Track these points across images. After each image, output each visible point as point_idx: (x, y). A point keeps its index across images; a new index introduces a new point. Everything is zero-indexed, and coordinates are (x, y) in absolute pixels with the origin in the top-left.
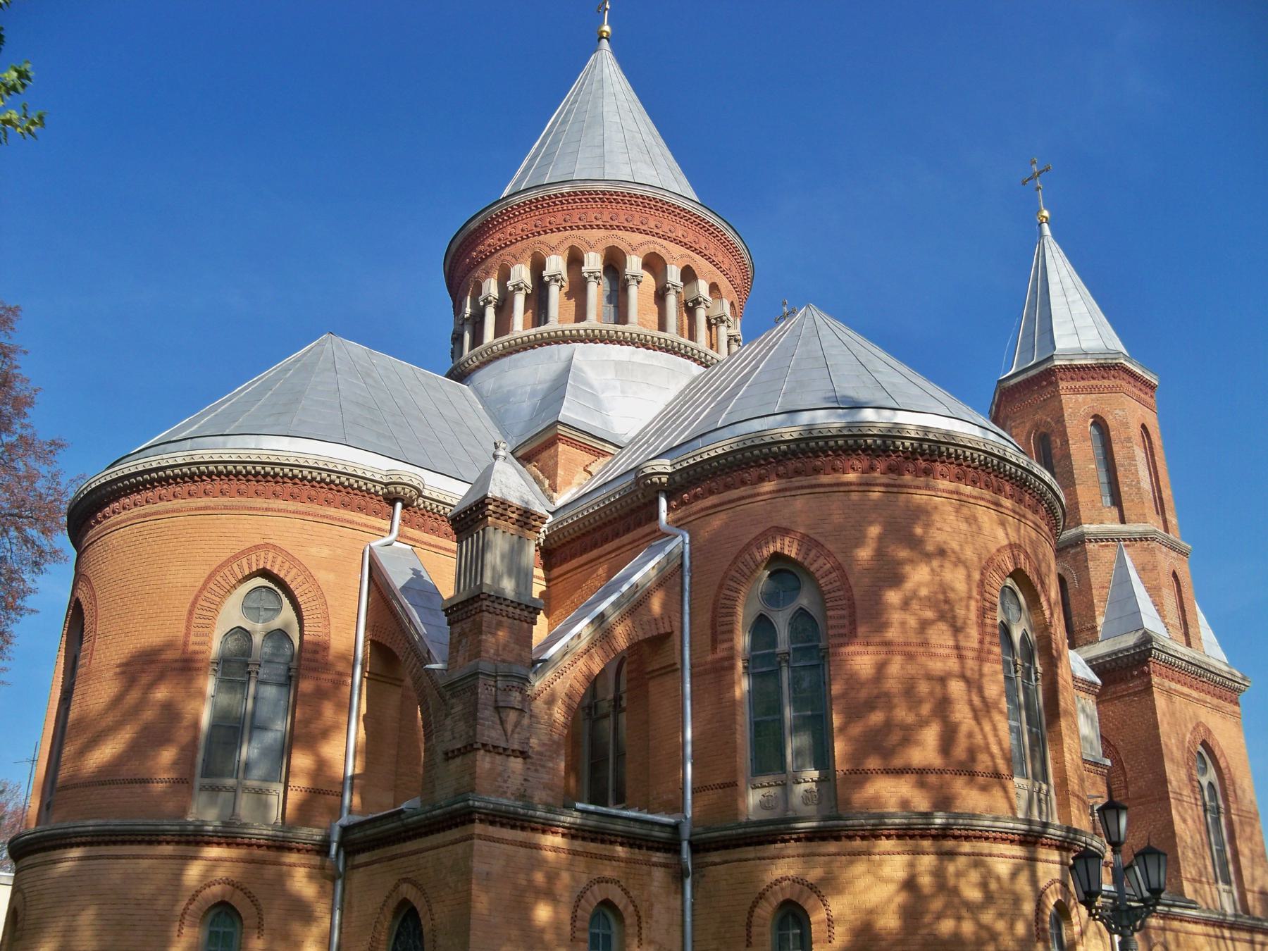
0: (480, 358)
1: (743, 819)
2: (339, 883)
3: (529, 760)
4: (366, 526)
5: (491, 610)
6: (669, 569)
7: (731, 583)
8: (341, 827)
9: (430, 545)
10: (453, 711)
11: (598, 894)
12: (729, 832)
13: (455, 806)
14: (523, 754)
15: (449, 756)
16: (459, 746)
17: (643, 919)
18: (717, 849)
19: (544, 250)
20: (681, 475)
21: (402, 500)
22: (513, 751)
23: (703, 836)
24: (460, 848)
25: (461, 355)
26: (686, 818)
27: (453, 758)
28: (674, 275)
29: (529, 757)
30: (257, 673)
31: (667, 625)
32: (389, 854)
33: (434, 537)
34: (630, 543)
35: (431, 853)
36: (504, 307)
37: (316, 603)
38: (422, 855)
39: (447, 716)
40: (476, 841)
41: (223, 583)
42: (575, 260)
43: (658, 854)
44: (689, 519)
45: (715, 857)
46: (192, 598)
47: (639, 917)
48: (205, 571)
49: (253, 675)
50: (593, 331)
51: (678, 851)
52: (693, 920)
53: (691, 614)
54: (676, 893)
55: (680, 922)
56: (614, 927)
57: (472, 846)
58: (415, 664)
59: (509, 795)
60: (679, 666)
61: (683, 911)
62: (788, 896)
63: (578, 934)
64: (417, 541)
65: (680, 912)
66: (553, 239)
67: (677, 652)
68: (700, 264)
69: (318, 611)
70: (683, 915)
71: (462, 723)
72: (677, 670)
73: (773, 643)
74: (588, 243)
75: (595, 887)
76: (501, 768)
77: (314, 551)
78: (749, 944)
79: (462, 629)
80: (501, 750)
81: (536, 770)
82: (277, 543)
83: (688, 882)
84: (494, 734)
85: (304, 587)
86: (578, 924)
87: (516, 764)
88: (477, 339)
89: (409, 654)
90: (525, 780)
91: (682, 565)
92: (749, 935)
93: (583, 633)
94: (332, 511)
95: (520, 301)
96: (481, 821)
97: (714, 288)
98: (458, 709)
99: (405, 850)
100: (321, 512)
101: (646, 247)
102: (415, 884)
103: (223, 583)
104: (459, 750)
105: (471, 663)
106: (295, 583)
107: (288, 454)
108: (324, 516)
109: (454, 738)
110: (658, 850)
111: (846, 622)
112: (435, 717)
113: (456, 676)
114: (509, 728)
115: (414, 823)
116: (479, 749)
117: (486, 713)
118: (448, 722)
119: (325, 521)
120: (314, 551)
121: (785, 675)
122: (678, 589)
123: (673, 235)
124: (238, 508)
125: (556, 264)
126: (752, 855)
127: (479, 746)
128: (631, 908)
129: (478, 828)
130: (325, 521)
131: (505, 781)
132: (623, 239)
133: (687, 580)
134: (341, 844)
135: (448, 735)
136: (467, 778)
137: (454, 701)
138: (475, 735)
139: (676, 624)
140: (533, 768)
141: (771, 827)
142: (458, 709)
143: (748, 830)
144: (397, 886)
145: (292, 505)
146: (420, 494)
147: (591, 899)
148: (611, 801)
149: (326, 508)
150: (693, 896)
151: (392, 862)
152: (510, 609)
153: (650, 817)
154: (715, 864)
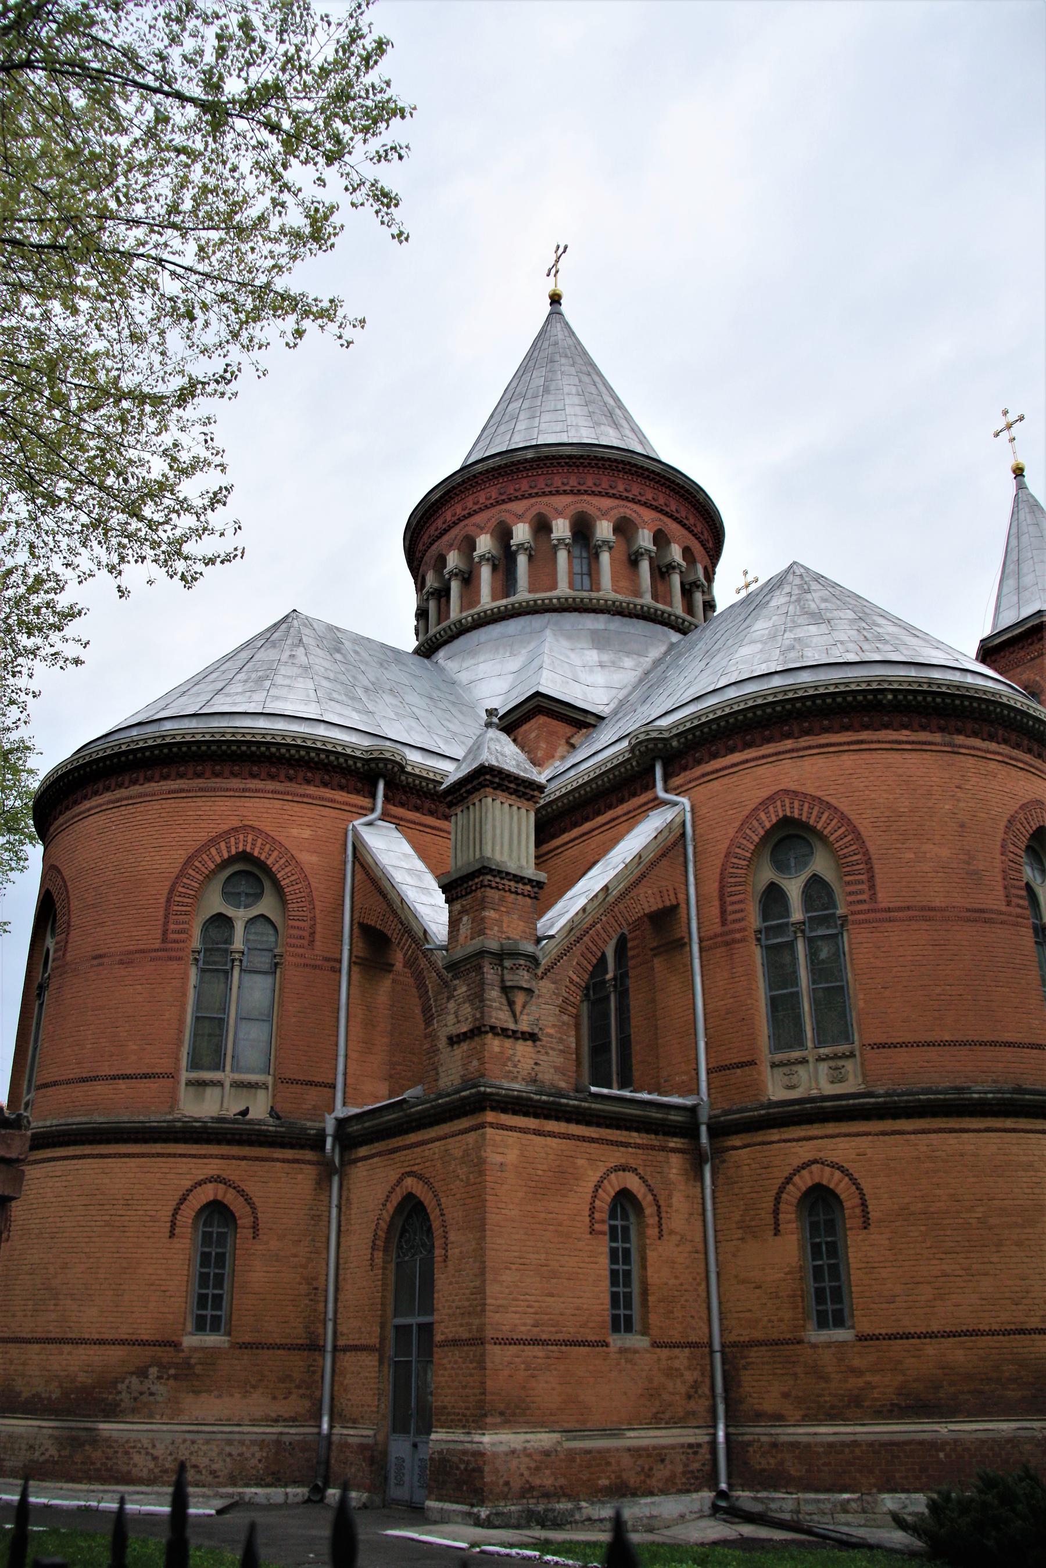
0: (449, 632)
1: (764, 1100)
2: (336, 1179)
3: (538, 1043)
4: (347, 804)
5: (494, 884)
6: (672, 838)
7: (737, 850)
8: (336, 1119)
9: (414, 823)
10: (455, 993)
12: (751, 1114)
13: (463, 1094)
14: (531, 1037)
15: (454, 1041)
16: (464, 1029)
17: (663, 1209)
19: (509, 519)
20: (678, 741)
21: (384, 777)
22: (523, 1033)
23: (722, 1119)
24: (471, 1137)
25: (448, 617)
26: (702, 1100)
27: (458, 1043)
28: (645, 539)
29: (539, 1040)
30: (241, 961)
31: (672, 896)
32: (390, 1147)
33: (418, 815)
34: (625, 814)
35: (438, 1143)
36: (469, 579)
37: (299, 886)
38: (430, 1146)
39: (449, 999)
40: (489, 1130)
41: (203, 869)
42: (542, 527)
43: (675, 1139)
44: (691, 785)
45: (736, 1141)
46: (168, 884)
47: (659, 1207)
48: (181, 856)
49: (237, 963)
50: (566, 599)
51: (696, 1136)
52: (714, 1209)
53: (697, 885)
54: (695, 1180)
55: (700, 1211)
56: (632, 1219)
57: (484, 1134)
58: (410, 946)
59: (520, 1078)
60: (686, 940)
61: (703, 1198)
62: (817, 1180)
63: (597, 1226)
64: (401, 819)
65: (700, 1201)
66: (518, 507)
67: (684, 925)
68: (673, 528)
69: (303, 894)
70: (703, 1204)
71: (467, 1005)
72: (685, 944)
73: (786, 912)
74: (556, 509)
75: (613, 1176)
76: (511, 1052)
77: (295, 832)
78: (777, 1232)
79: (463, 906)
80: (510, 1033)
81: (547, 1053)
82: (255, 824)
85: (287, 870)
86: (597, 1215)
87: (523, 1050)
88: (443, 613)
89: (403, 935)
90: (536, 1064)
91: (683, 835)
92: (777, 1224)
93: (588, 907)
94: (311, 790)
95: (485, 572)
96: (493, 1109)
97: (687, 552)
98: (462, 990)
99: (408, 1142)
100: (301, 791)
101: (616, 511)
102: (420, 1177)
103: (203, 869)
104: (465, 1033)
105: (474, 941)
106: (277, 866)
107: (264, 731)
108: (304, 796)
109: (459, 1022)
110: (675, 1135)
111: (864, 887)
112: (435, 1001)
113: (459, 953)
114: (518, 1008)
115: (418, 1112)
116: (487, 1032)
117: (494, 994)
118: (451, 1005)
119: (305, 800)
120: (295, 832)
121: (801, 947)
122: (681, 859)
123: (643, 499)
124: (214, 790)
125: (521, 533)
126: (776, 1138)
127: (488, 1029)
128: (650, 1197)
129: (490, 1116)
130: (305, 800)
131: (515, 1066)
132: (591, 504)
133: (690, 850)
134: (336, 1137)
135: (451, 1019)
136: (475, 1063)
137: (456, 982)
138: (482, 1017)
139: (682, 897)
140: (543, 1051)
141: (797, 1107)
142: (462, 990)
143: (771, 1111)
144: (400, 1181)
145: (271, 785)
146: (402, 768)
147: (609, 1188)
148: (615, 1084)
149: (306, 787)
150: (713, 1183)
151: (393, 1156)
152: (512, 884)
153: (665, 1099)
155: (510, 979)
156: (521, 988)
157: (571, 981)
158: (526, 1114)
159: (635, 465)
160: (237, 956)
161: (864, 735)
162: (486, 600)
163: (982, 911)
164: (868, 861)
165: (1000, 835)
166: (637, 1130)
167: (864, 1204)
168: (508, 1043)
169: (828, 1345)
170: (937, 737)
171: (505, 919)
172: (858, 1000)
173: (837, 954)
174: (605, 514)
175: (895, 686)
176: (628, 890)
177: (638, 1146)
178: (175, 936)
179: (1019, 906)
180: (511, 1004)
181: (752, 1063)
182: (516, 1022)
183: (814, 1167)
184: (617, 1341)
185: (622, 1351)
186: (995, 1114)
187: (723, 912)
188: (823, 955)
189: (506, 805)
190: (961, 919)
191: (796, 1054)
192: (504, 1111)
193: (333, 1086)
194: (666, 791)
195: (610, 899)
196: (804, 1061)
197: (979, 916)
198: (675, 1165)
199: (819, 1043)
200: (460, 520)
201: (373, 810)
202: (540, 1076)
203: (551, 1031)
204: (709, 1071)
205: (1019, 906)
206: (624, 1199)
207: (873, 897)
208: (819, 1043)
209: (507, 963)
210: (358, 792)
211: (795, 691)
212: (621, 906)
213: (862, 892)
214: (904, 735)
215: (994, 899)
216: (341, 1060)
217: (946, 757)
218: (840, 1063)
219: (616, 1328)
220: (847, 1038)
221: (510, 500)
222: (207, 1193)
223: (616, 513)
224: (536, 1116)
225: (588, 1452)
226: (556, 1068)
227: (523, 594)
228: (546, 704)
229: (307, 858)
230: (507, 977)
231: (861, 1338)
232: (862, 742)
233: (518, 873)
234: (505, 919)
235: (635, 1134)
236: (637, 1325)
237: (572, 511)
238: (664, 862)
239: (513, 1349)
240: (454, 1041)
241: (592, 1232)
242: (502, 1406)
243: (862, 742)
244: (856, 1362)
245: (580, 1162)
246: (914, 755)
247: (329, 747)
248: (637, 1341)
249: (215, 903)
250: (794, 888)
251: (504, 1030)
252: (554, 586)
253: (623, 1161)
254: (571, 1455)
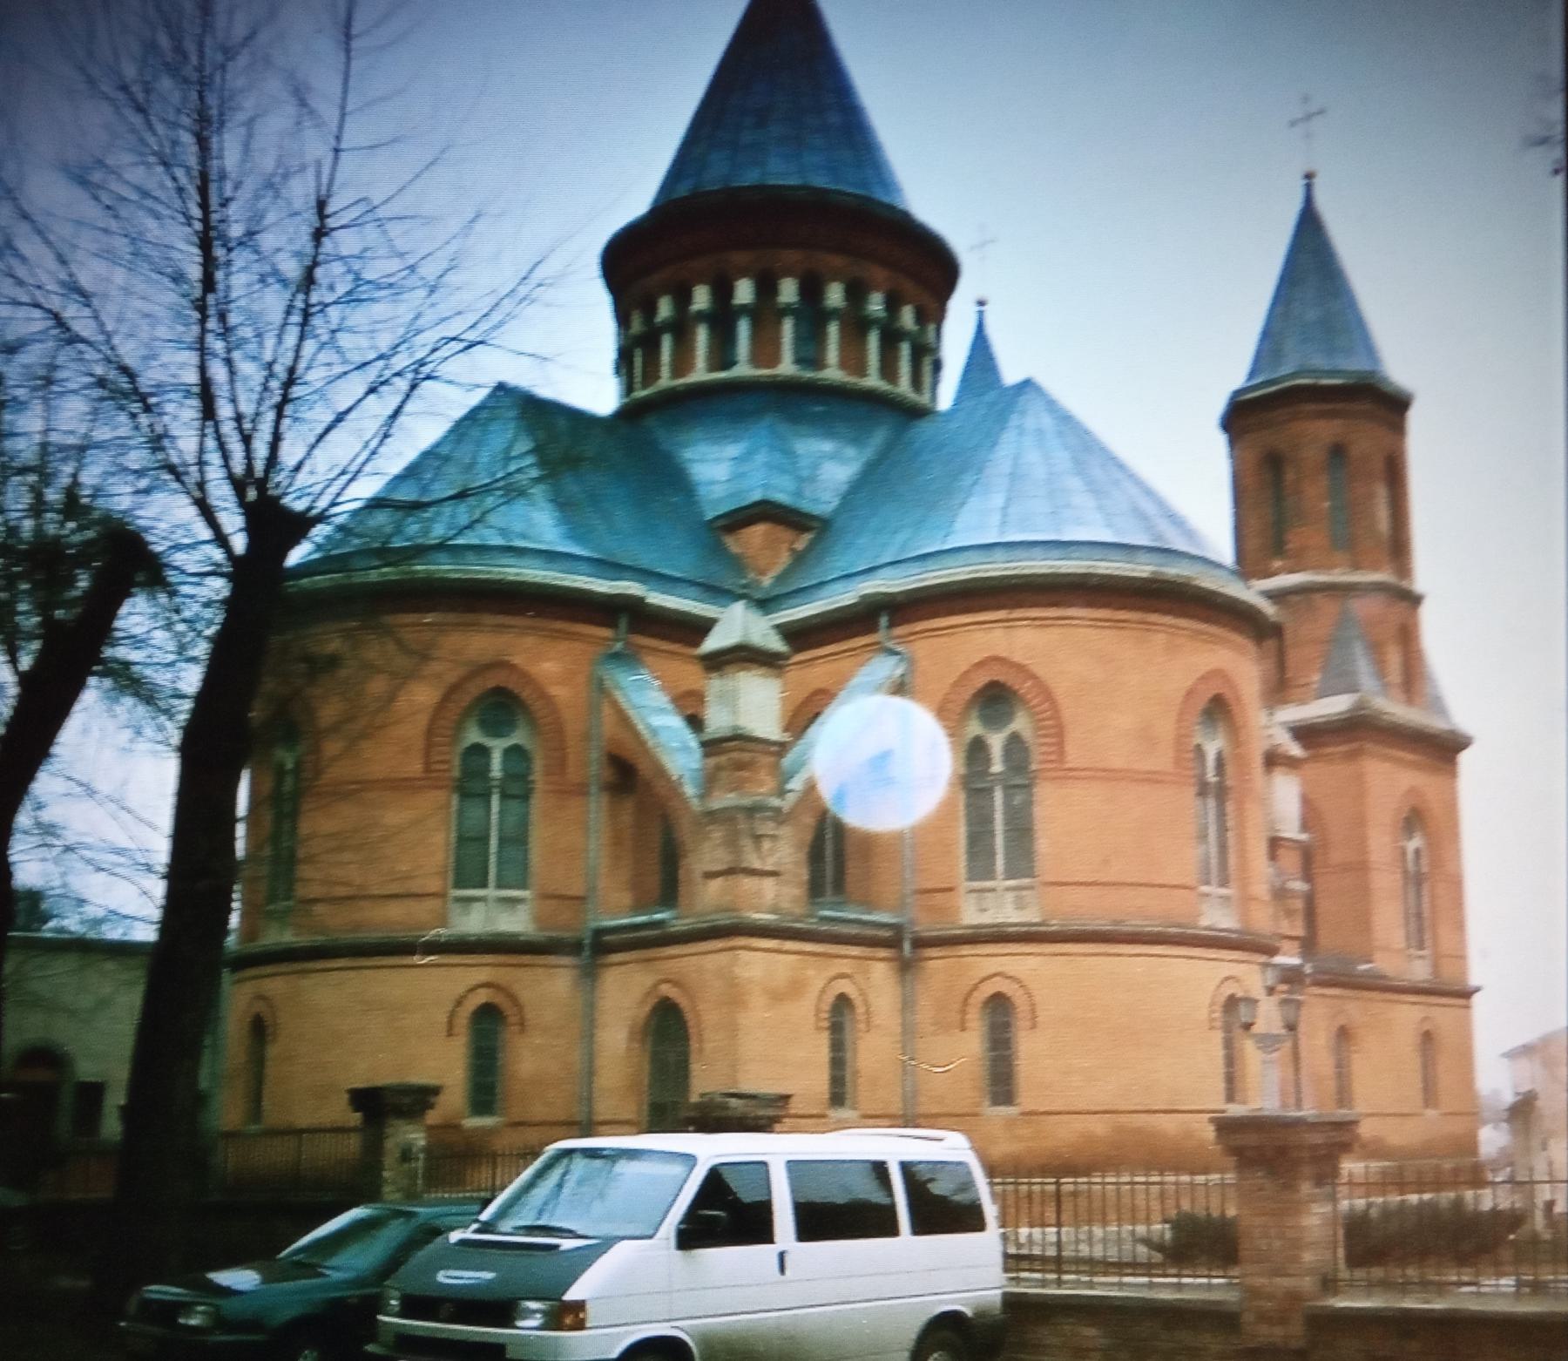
73: (988, 761)
88: (651, 374)
121: (998, 796)
144: (655, 986)
156: (767, 836)
160: (495, 783)
162: (700, 373)
167: (1033, 1011)
172: (1043, 844)
173: (1029, 804)
178: (438, 767)
181: (950, 889)
206: (843, 1002)
215: (1163, 760)
222: (482, 997)
227: (743, 369)
229: (559, 692)
249: (474, 736)
250: (996, 742)
252: (774, 360)
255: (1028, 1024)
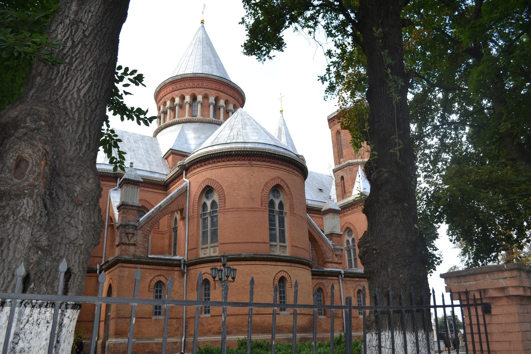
6: (183, 191)
11: (157, 279)
14: (134, 245)
18: (192, 266)
22: (131, 244)
42: (183, 98)
45: (191, 268)
83: (185, 275)
84: (125, 240)
86: (151, 287)
87: (132, 248)
91: (187, 190)
110: (177, 267)
111: (223, 203)
114: (130, 238)
126: (198, 267)
132: (196, 91)
139: (185, 206)
152: (131, 207)
154: (191, 270)
155: (128, 231)
156: (130, 233)
157: (148, 230)
158: (131, 263)
159: (209, 78)
161: (227, 163)
163: (254, 208)
164: (224, 196)
165: (262, 188)
166: (165, 266)
168: (127, 246)
169: (205, 318)
170: (247, 162)
171: (128, 216)
174: (200, 93)
175: (235, 150)
176: (167, 206)
177: (164, 270)
179: (265, 206)
180: (128, 237)
182: (129, 241)
183: (205, 274)
184: (154, 318)
185: (156, 320)
186: (250, 260)
187: (193, 210)
188: (215, 220)
189: (131, 188)
190: (247, 210)
191: (206, 246)
192: (125, 263)
193: (102, 257)
194: (186, 178)
195: (162, 208)
196: (207, 248)
197: (253, 210)
198: (176, 274)
199: (212, 243)
200: (164, 97)
201: (116, 186)
202: (136, 254)
203: (140, 243)
204: (188, 251)
205: (265, 206)
207: (225, 206)
208: (212, 243)
209: (127, 227)
210: (112, 182)
211: (210, 152)
212: (165, 210)
213: (222, 204)
214: (238, 162)
215: (257, 205)
216: (104, 250)
217: (249, 167)
218: (215, 248)
219: (156, 314)
220: (217, 241)
221: (175, 91)
223: (203, 93)
224: (134, 264)
225: (143, 343)
226: (141, 252)
228: (174, 151)
230: (127, 230)
231: (212, 316)
232: (227, 165)
233: (132, 204)
234: (128, 216)
235: (164, 267)
236: (162, 313)
237: (190, 94)
238: (180, 198)
239: (123, 319)
240: (118, 246)
241: (149, 291)
242: (119, 333)
243: (227, 165)
244: (211, 322)
245: (146, 274)
246: (240, 167)
247: (103, 171)
248: (161, 317)
251: (126, 244)
253: (160, 274)
254: (138, 344)
255: (213, 288)
